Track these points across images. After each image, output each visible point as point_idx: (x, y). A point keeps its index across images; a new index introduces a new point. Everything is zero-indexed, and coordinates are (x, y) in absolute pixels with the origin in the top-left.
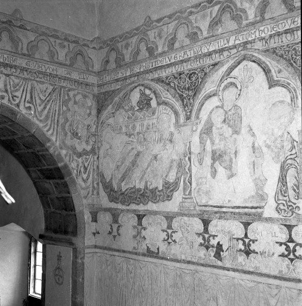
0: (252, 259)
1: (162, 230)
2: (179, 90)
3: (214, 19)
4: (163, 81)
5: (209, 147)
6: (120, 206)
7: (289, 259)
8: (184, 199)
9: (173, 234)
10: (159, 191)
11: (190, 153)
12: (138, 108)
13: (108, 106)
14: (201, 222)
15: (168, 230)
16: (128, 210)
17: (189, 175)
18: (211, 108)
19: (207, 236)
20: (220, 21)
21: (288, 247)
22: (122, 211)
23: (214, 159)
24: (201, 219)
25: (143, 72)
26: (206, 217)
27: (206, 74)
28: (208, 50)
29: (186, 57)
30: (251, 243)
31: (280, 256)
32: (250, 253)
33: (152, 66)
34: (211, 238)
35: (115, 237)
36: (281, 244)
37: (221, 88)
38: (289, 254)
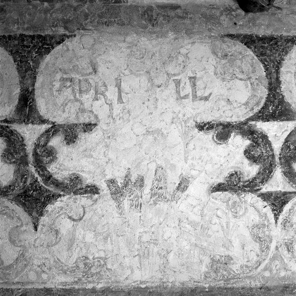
0: (65, 226)
7: (266, 197)
21: (258, 139)
30: (56, 142)
31: (219, 188)
32: (52, 198)
36: (223, 131)
38: (266, 174)
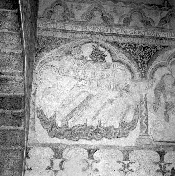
1: (118, 162)
2: (135, 55)
3: (163, 18)
4: (119, 45)
5: (163, 100)
6: (65, 141)
8: (140, 136)
9: (130, 165)
10: (114, 129)
11: (146, 102)
12: (91, 59)
13: (52, 49)
14: (157, 153)
15: (124, 162)
16: (76, 145)
17: (145, 118)
18: (163, 74)
19: (163, 164)
20: (169, 22)
22: (68, 146)
23: (166, 108)
24: (157, 151)
25: (96, 32)
26: (161, 149)
27: (157, 50)
28: (159, 36)
29: (140, 34)
33: (107, 31)
34: (167, 166)
35: (56, 172)
37: (170, 63)
